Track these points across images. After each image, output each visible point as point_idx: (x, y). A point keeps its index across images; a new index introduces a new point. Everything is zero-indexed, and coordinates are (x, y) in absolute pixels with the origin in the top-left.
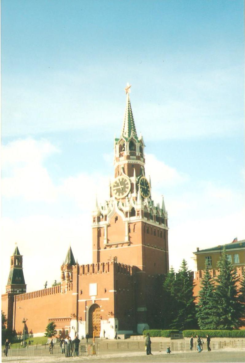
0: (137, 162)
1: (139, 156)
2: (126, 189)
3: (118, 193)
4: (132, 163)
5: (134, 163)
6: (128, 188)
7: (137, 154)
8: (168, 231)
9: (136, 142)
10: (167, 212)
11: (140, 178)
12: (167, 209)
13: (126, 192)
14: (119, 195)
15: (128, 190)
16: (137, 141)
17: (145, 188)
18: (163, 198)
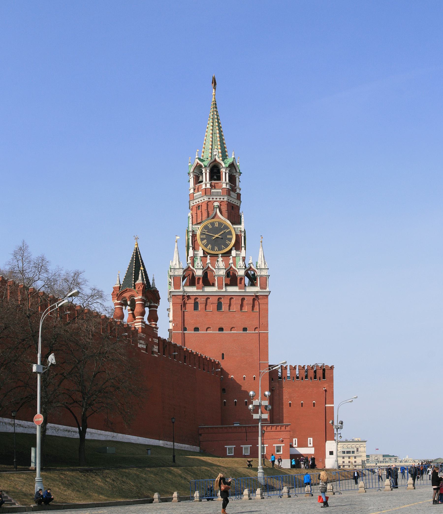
2: (228, 242)
3: (210, 246)
7: (238, 191)
14: (213, 249)
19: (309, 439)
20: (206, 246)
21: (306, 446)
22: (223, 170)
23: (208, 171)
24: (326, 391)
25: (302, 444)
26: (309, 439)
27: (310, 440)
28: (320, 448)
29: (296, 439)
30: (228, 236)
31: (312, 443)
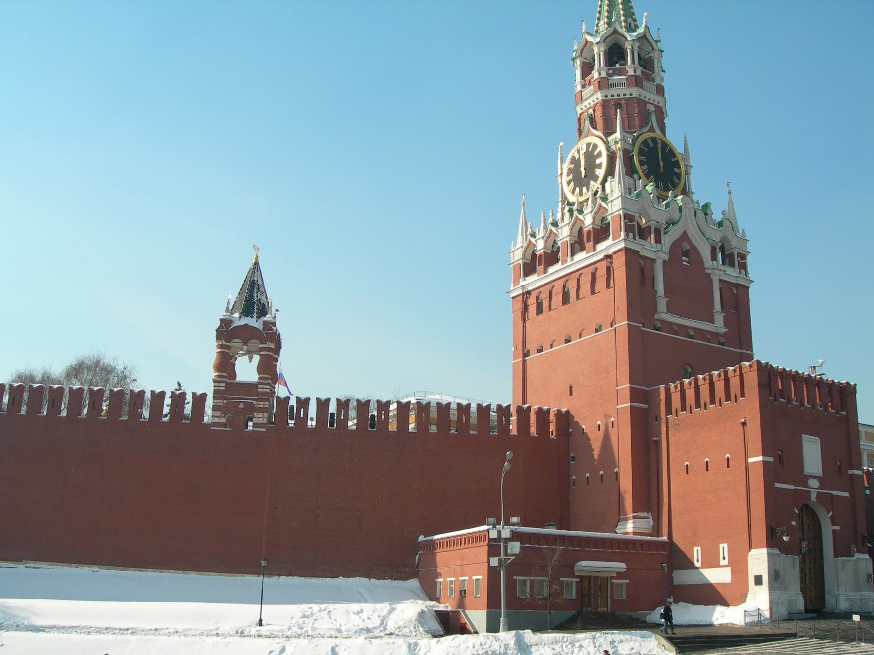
0: (631, 94)
1: (636, 77)
3: (577, 190)
4: (616, 97)
5: (622, 97)
6: (599, 166)
7: (631, 72)
8: (751, 291)
9: (626, 39)
10: (743, 233)
11: (638, 136)
12: (742, 224)
13: (596, 178)
14: (581, 194)
15: (600, 173)
16: (629, 38)
17: (658, 164)
18: (730, 193)
19: (721, 546)
20: (573, 193)
21: (717, 565)
22: (596, 51)
23: (578, 63)
24: (744, 424)
25: (712, 562)
26: (721, 546)
27: (724, 547)
28: (739, 566)
29: (699, 548)
30: (598, 161)
31: (726, 556)
